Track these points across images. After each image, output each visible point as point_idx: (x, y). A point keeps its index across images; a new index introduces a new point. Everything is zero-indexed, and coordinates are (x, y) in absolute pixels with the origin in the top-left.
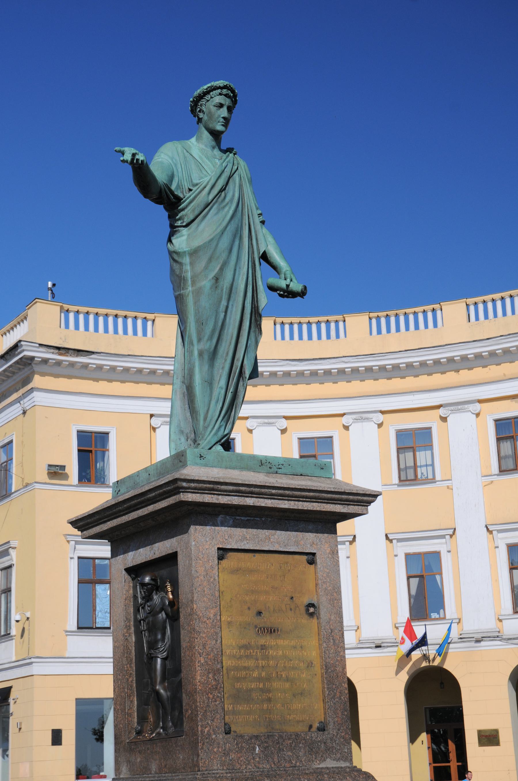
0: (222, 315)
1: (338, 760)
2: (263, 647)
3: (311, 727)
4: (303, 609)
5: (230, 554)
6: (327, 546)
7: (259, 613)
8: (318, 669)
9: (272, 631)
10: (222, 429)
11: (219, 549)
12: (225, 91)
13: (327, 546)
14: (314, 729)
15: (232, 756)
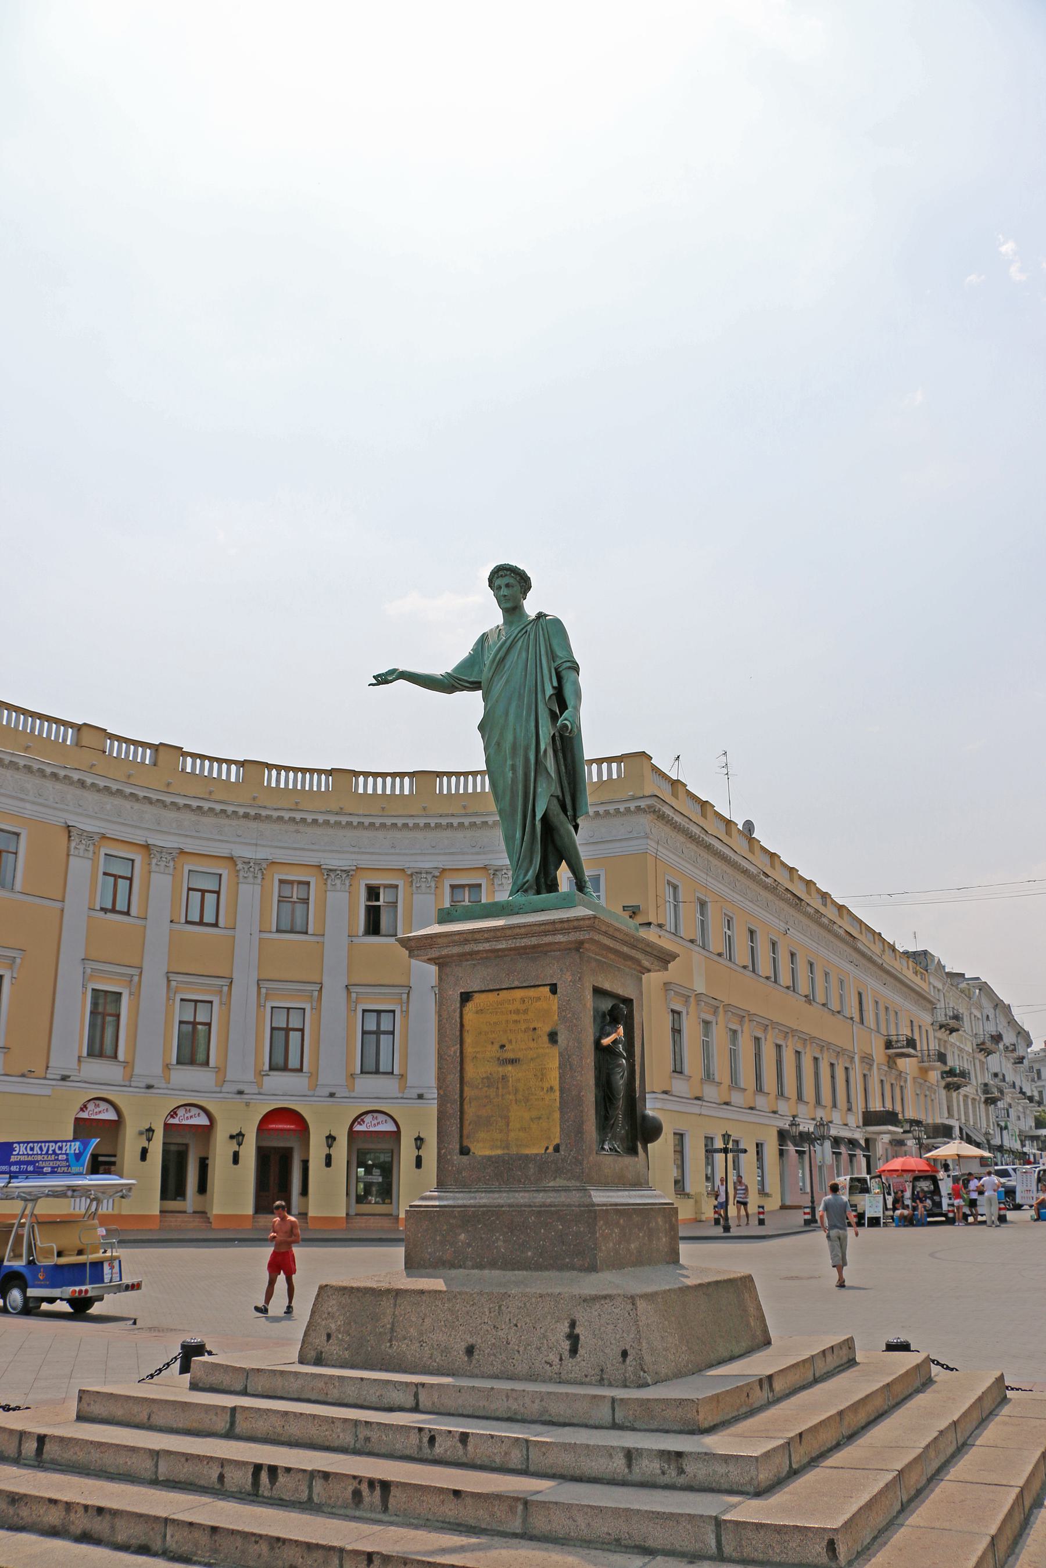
0: (510, 774)
1: (569, 1179)
2: (504, 1077)
3: (547, 1148)
4: (546, 1038)
5: (476, 995)
6: (569, 974)
7: (502, 1046)
8: (557, 1093)
9: (512, 1061)
10: (521, 877)
11: (462, 993)
12: (500, 573)
13: (569, 974)
14: (551, 1150)
15: (464, 1174)
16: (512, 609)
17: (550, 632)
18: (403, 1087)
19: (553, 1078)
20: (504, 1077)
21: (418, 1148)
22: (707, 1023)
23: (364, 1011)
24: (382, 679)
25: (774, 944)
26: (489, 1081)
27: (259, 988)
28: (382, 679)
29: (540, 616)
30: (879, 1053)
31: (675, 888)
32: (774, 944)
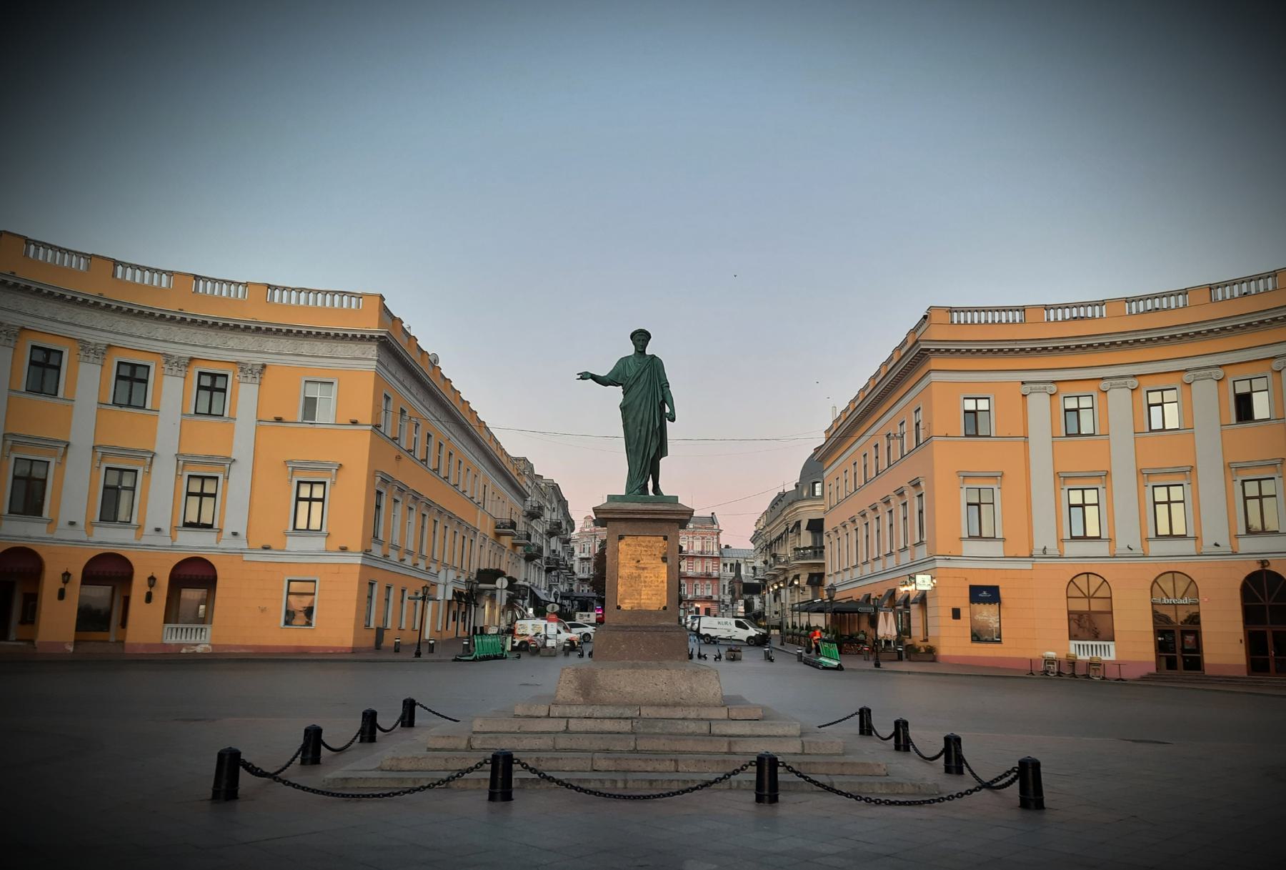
16: (640, 350)
17: (655, 365)
18: (138, 537)
19: (664, 576)
20: (639, 576)
21: (151, 586)
22: (396, 501)
23: (107, 468)
24: (584, 376)
25: (441, 445)
26: (631, 576)
27: (4, 440)
28: (584, 376)
29: (653, 357)
30: (489, 530)
31: (387, 398)
32: (441, 445)
